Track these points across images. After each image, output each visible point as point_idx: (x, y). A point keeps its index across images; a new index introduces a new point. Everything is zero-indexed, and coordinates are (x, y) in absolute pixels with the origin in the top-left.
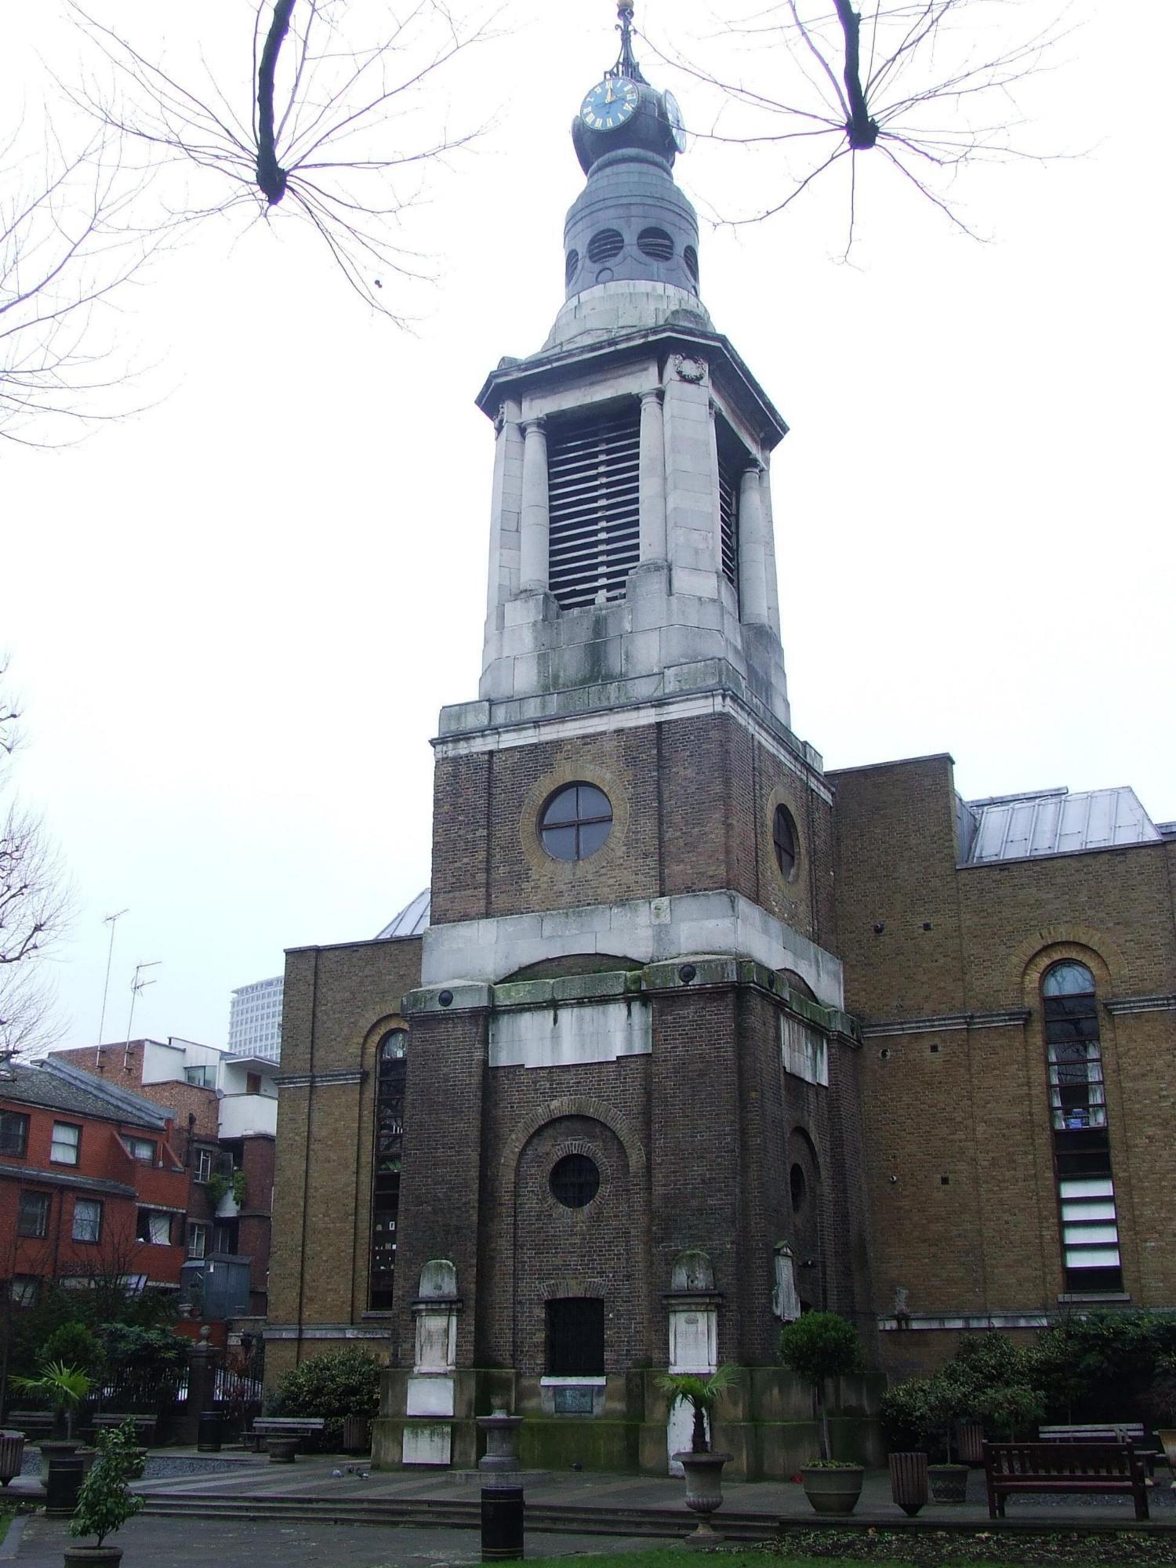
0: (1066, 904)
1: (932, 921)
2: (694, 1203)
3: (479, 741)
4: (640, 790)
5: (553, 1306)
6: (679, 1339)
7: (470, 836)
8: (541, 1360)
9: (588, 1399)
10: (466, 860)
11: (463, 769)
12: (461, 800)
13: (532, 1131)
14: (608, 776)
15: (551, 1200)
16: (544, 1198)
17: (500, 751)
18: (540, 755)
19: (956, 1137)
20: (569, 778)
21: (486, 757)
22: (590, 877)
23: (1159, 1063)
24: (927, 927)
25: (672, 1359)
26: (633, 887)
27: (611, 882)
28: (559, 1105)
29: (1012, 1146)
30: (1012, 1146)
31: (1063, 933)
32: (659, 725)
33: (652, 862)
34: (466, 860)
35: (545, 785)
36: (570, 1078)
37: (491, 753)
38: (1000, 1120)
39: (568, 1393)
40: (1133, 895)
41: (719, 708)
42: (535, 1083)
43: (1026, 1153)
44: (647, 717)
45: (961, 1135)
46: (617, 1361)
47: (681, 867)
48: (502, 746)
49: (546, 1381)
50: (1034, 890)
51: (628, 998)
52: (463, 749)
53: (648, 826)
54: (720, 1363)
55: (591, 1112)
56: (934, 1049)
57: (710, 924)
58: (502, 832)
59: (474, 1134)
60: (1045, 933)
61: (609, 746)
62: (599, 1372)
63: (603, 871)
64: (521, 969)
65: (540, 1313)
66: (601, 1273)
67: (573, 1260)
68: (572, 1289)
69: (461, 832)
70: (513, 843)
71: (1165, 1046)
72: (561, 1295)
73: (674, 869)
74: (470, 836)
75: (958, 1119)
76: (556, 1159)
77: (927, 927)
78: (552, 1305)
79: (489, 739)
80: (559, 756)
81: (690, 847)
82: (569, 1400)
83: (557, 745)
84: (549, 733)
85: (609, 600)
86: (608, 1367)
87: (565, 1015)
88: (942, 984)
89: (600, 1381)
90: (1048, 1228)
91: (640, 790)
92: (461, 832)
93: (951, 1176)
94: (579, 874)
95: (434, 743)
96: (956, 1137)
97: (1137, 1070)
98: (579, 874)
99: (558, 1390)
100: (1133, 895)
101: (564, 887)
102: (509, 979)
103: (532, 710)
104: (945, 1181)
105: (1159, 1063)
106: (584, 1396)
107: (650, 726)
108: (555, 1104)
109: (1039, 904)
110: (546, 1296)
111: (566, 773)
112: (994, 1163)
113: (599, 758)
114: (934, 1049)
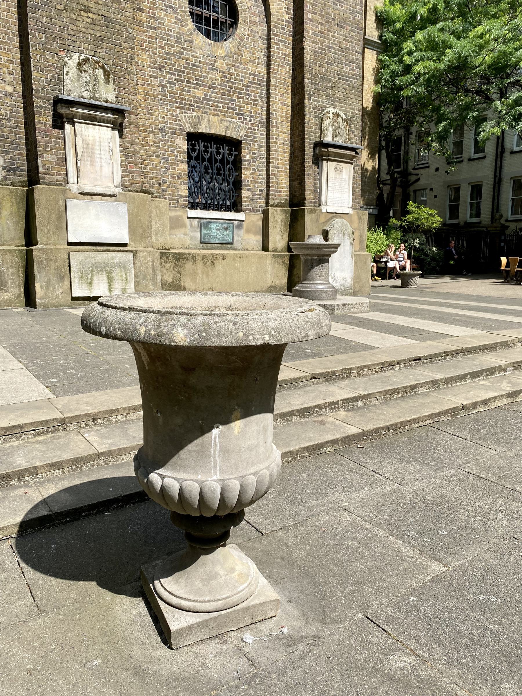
2: (336, 67)
5: (193, 138)
6: (330, 184)
9: (229, 232)
15: (191, 25)
39: (213, 226)
46: (252, 200)
49: (193, 213)
62: (236, 207)
65: (183, 144)
66: (240, 115)
67: (214, 95)
68: (213, 125)
72: (203, 129)
78: (193, 138)
82: (214, 233)
86: (244, 205)
89: (240, 216)
99: (204, 223)
106: (226, 229)
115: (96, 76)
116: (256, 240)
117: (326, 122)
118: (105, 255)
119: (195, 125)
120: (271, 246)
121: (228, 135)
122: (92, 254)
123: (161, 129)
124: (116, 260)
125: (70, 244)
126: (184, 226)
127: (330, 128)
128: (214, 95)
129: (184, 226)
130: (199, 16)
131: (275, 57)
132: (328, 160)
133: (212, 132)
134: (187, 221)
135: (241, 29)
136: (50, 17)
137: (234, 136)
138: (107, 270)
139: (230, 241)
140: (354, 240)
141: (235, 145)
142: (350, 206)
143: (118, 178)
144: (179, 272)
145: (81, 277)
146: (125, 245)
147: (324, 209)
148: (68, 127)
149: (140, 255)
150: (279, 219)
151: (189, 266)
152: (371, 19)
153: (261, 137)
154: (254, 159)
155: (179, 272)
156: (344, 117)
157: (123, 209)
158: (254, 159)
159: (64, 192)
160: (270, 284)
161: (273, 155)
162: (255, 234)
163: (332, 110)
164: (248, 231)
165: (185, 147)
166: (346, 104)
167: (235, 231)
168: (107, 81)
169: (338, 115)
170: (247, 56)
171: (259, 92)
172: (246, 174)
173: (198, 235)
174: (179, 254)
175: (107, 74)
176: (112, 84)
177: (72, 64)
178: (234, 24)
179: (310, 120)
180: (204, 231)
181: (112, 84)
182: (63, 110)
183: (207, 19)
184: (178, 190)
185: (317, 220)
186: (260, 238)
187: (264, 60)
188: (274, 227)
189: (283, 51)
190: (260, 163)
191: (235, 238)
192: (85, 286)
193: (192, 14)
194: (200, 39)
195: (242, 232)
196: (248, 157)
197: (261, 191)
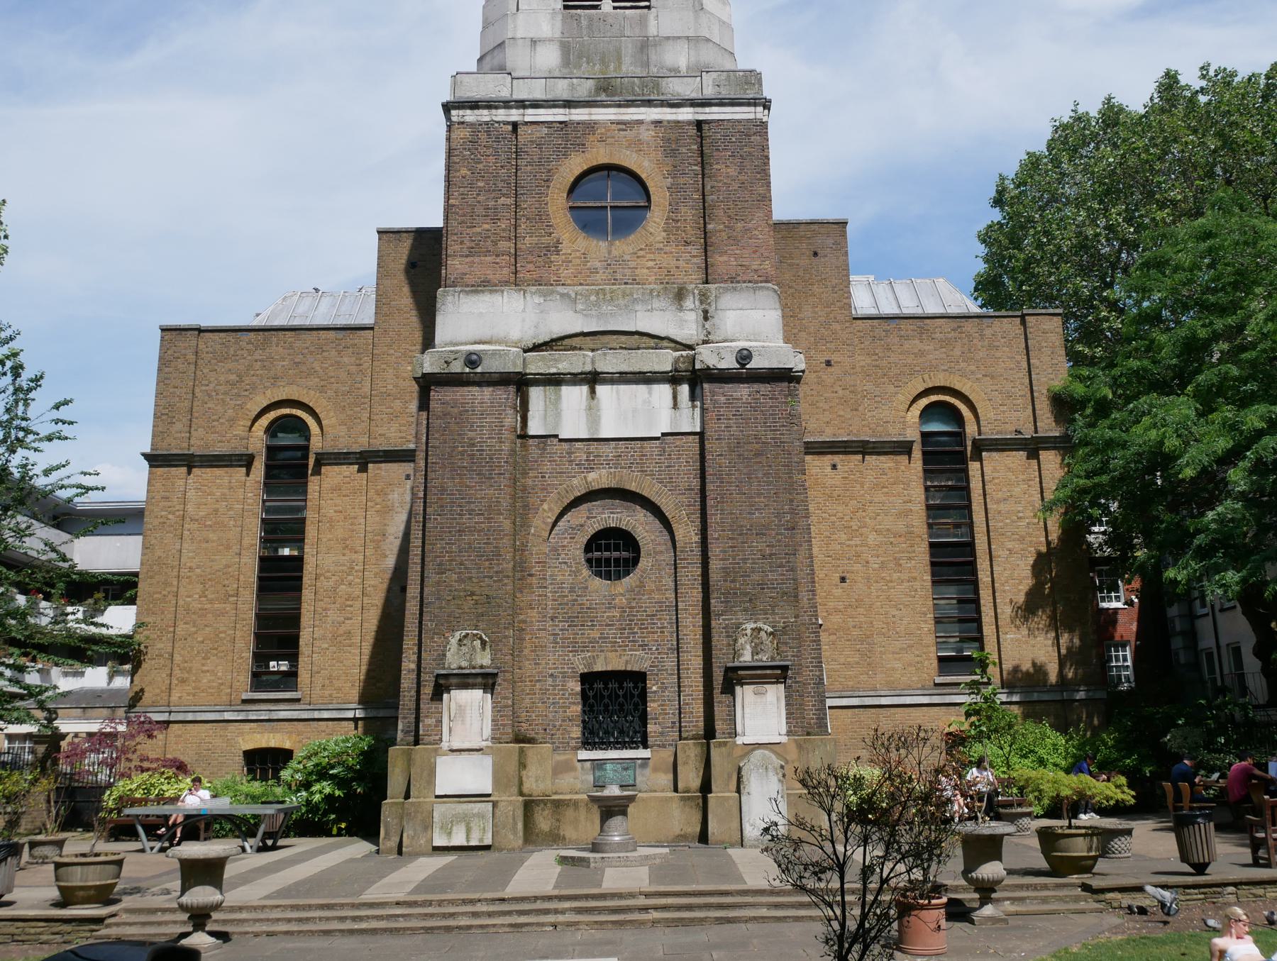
0: (944, 356)
1: (834, 358)
2: (756, 577)
3: (501, 111)
4: (681, 181)
5: (588, 679)
7: (492, 203)
8: (576, 732)
9: (630, 772)
10: (486, 226)
11: (483, 136)
12: (480, 166)
13: (566, 502)
14: (646, 164)
15: (586, 572)
16: (579, 571)
17: (526, 123)
18: (570, 136)
19: (852, 543)
20: (603, 159)
21: (510, 128)
22: (627, 257)
23: (1017, 491)
24: (828, 363)
25: (739, 729)
26: (673, 271)
27: (651, 264)
28: (599, 478)
29: (899, 552)
30: (899, 552)
31: (940, 380)
32: (699, 124)
33: (696, 250)
34: (486, 226)
35: (575, 165)
36: (608, 450)
37: (515, 125)
38: (888, 530)
39: (609, 766)
40: (998, 354)
41: (759, 116)
42: (570, 453)
43: (910, 559)
44: (686, 114)
45: (857, 541)
46: (662, 734)
47: (725, 258)
48: (527, 119)
49: (584, 754)
50: (917, 342)
51: (673, 379)
52: (484, 115)
53: (689, 213)
54: (789, 733)
55: (633, 487)
56: (834, 467)
57: (756, 315)
58: (528, 203)
59: (505, 503)
60: (926, 377)
61: (647, 134)
63: (641, 253)
64: (552, 340)
67: (610, 632)
69: (480, 198)
70: (541, 217)
71: (1021, 477)
72: (599, 667)
73: (717, 259)
74: (492, 203)
75: (855, 527)
76: (591, 532)
77: (828, 363)
78: (588, 679)
79: (514, 111)
80: (591, 138)
81: (735, 240)
83: (590, 126)
84: (579, 115)
85: (615, 8)
86: (651, 741)
87: (600, 389)
88: (842, 413)
89: (645, 753)
90: (925, 622)
91: (681, 181)
92: (480, 198)
93: (848, 575)
94: (615, 253)
95: (447, 108)
96: (852, 543)
97: (1000, 495)
98: (615, 253)
99: (598, 765)
100: (998, 354)
101: (598, 265)
102: (536, 348)
103: (561, 90)
104: (843, 580)
105: (1017, 491)
106: (626, 769)
107: (689, 123)
108: (592, 476)
109: (922, 353)
110: (582, 669)
111: (601, 156)
112: (883, 566)
113: (637, 145)
114: (834, 467)
115: (474, 648)
116: (665, 779)
117: (741, 640)
118: (465, 806)
119: (590, 665)
120: (680, 786)
121: (629, 668)
122: (453, 806)
123: (552, 675)
124: (475, 811)
125: (437, 797)
126: (573, 769)
127: (748, 647)
128: (610, 632)
129: (573, 769)
130: (599, 561)
131: (683, 580)
132: (742, 685)
133: (610, 668)
134: (579, 765)
135: (644, 563)
136: (441, 608)
137: (636, 668)
138: (466, 820)
139: (631, 782)
140: (784, 776)
141: (639, 678)
142: (784, 731)
143: (487, 732)
144: (558, 820)
145: (442, 828)
146: (489, 795)
147: (739, 740)
148: (445, 696)
149: (501, 805)
150: (690, 752)
151: (570, 813)
152: (1044, 407)
153: (670, 664)
154: (663, 688)
155: (558, 820)
156: (770, 630)
157: (487, 762)
158: (663, 688)
159: (436, 750)
160: (678, 832)
161: (685, 682)
162: (666, 772)
163: (750, 626)
164: (655, 770)
165: (578, 689)
166: (774, 613)
167: (638, 771)
168: (483, 648)
169: (760, 629)
170: (650, 586)
171: (667, 619)
172: (652, 707)
173: (591, 778)
174: (559, 801)
175: (484, 643)
176: (488, 650)
177: (454, 641)
178: (636, 561)
179: (719, 640)
180: (598, 774)
181: (488, 650)
182: (442, 681)
183: (608, 561)
184: (569, 733)
185: (729, 754)
186: (671, 776)
187: (672, 585)
188: (685, 763)
189: (691, 574)
190: (671, 693)
191: (639, 779)
192: (444, 836)
193: (589, 561)
194: (598, 582)
195: (648, 771)
196: (654, 688)
197: (674, 723)
